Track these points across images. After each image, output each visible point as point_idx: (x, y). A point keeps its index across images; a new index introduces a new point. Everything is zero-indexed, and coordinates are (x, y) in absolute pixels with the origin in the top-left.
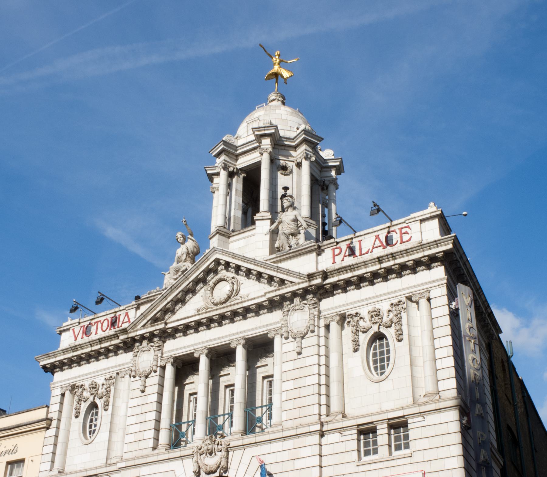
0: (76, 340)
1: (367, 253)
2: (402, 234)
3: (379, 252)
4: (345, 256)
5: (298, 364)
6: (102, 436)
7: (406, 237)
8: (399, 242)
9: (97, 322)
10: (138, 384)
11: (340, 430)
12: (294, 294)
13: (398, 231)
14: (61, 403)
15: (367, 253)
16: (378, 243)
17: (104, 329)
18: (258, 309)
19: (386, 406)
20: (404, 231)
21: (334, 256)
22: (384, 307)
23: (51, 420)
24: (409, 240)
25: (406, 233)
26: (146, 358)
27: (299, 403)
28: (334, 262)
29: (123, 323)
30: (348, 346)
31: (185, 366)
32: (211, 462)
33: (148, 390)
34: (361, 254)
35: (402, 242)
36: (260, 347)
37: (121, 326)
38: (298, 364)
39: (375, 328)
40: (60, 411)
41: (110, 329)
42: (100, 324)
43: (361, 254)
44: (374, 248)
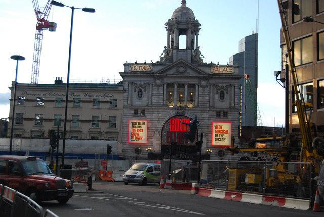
3: (224, 72)
5: (203, 94)
6: (145, 99)
7: (231, 70)
10: (157, 88)
11: (213, 111)
12: (204, 77)
14: (128, 86)
18: (192, 77)
19: (224, 107)
22: (225, 85)
23: (125, 90)
26: (159, 82)
27: (203, 102)
30: (215, 91)
31: (169, 85)
32: (180, 111)
33: (160, 90)
36: (192, 86)
38: (203, 94)
39: (222, 90)
40: (128, 89)
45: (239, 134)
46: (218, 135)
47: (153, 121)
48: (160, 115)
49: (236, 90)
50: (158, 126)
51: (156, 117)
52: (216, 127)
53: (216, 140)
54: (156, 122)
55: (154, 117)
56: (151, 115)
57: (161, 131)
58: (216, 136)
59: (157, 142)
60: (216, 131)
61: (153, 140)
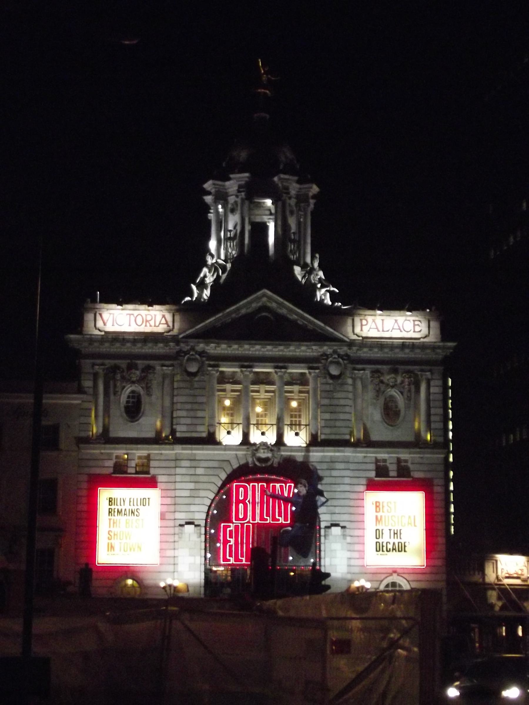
0: (105, 324)
1: (388, 331)
2: (414, 325)
4: (370, 328)
8: (413, 330)
9: (130, 315)
13: (412, 322)
15: (388, 331)
16: (396, 327)
17: (139, 323)
20: (417, 323)
21: (362, 325)
24: (420, 331)
25: (418, 325)
28: (362, 330)
29: (160, 324)
34: (383, 331)
35: (414, 332)
37: (158, 326)
41: (146, 326)
42: (133, 318)
43: (383, 331)
44: (393, 329)
45: (449, 530)
46: (386, 533)
47: (178, 493)
48: (200, 471)
49: (432, 390)
50: (193, 508)
51: (187, 478)
52: (377, 505)
53: (379, 548)
54: (187, 493)
55: (178, 478)
56: (172, 471)
57: (203, 523)
58: (378, 534)
59: (191, 560)
60: (378, 520)
61: (177, 553)
